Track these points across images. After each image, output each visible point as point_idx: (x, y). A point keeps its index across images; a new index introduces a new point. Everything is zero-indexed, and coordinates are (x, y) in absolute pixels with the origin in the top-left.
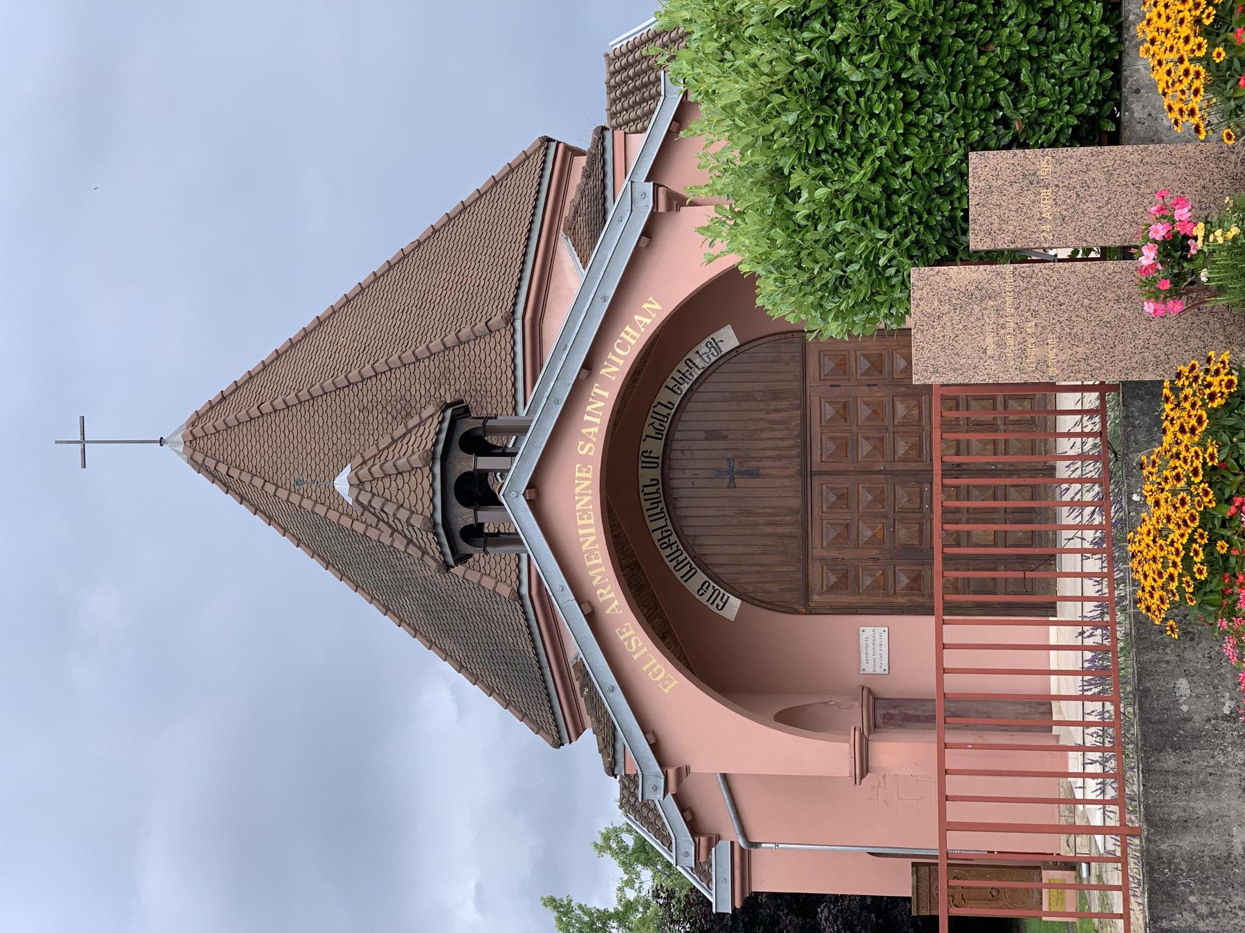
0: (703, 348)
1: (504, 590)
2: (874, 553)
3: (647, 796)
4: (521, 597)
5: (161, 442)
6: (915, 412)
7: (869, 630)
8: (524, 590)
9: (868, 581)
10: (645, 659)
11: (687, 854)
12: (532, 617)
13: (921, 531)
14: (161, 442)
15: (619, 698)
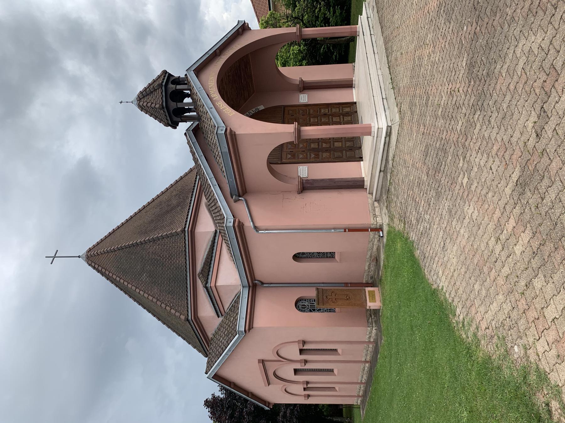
0: (254, 110)
1: (179, 230)
2: (304, 150)
3: (218, 132)
4: (184, 230)
5: (79, 257)
6: (316, 120)
7: (301, 167)
8: (186, 229)
9: (301, 156)
10: (224, 109)
11: (230, 222)
12: (188, 270)
13: (318, 145)
14: (79, 257)
15: (214, 110)
